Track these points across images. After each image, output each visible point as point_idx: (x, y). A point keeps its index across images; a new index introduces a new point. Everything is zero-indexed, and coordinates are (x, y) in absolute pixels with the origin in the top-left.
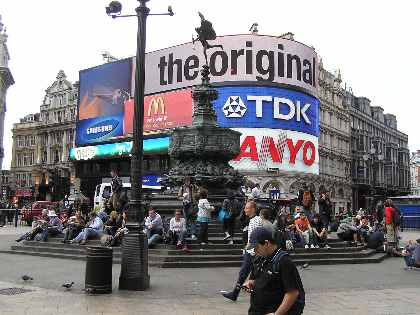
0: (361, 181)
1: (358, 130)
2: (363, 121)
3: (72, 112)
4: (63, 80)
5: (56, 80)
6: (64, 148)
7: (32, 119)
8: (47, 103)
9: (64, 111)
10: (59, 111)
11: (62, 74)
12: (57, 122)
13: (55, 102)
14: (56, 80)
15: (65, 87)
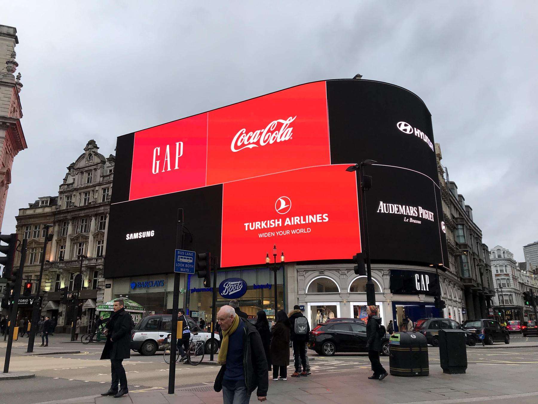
0: (467, 281)
1: (456, 219)
2: (457, 209)
3: (104, 192)
4: (93, 152)
5: (84, 152)
6: (91, 238)
7: (47, 202)
8: (70, 180)
9: (93, 191)
10: (86, 190)
11: (92, 144)
12: (82, 204)
13: (81, 181)
14: (84, 152)
15: (96, 160)
